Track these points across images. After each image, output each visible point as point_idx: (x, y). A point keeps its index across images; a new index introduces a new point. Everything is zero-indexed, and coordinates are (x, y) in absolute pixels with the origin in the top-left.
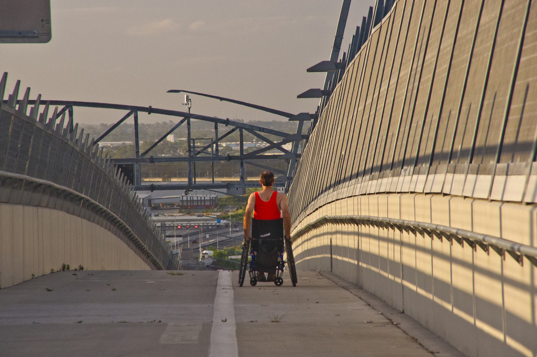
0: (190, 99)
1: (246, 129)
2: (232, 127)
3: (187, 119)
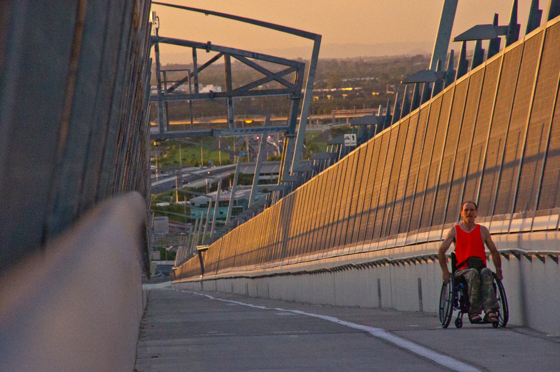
0: (158, 17)
1: (234, 56)
2: (216, 53)
3: (155, 43)
